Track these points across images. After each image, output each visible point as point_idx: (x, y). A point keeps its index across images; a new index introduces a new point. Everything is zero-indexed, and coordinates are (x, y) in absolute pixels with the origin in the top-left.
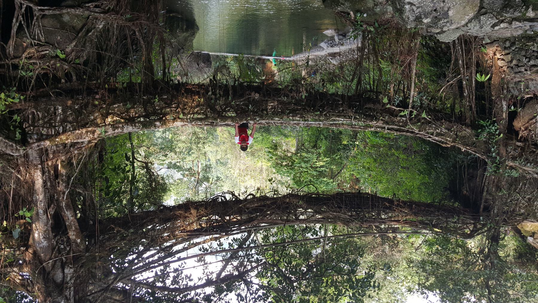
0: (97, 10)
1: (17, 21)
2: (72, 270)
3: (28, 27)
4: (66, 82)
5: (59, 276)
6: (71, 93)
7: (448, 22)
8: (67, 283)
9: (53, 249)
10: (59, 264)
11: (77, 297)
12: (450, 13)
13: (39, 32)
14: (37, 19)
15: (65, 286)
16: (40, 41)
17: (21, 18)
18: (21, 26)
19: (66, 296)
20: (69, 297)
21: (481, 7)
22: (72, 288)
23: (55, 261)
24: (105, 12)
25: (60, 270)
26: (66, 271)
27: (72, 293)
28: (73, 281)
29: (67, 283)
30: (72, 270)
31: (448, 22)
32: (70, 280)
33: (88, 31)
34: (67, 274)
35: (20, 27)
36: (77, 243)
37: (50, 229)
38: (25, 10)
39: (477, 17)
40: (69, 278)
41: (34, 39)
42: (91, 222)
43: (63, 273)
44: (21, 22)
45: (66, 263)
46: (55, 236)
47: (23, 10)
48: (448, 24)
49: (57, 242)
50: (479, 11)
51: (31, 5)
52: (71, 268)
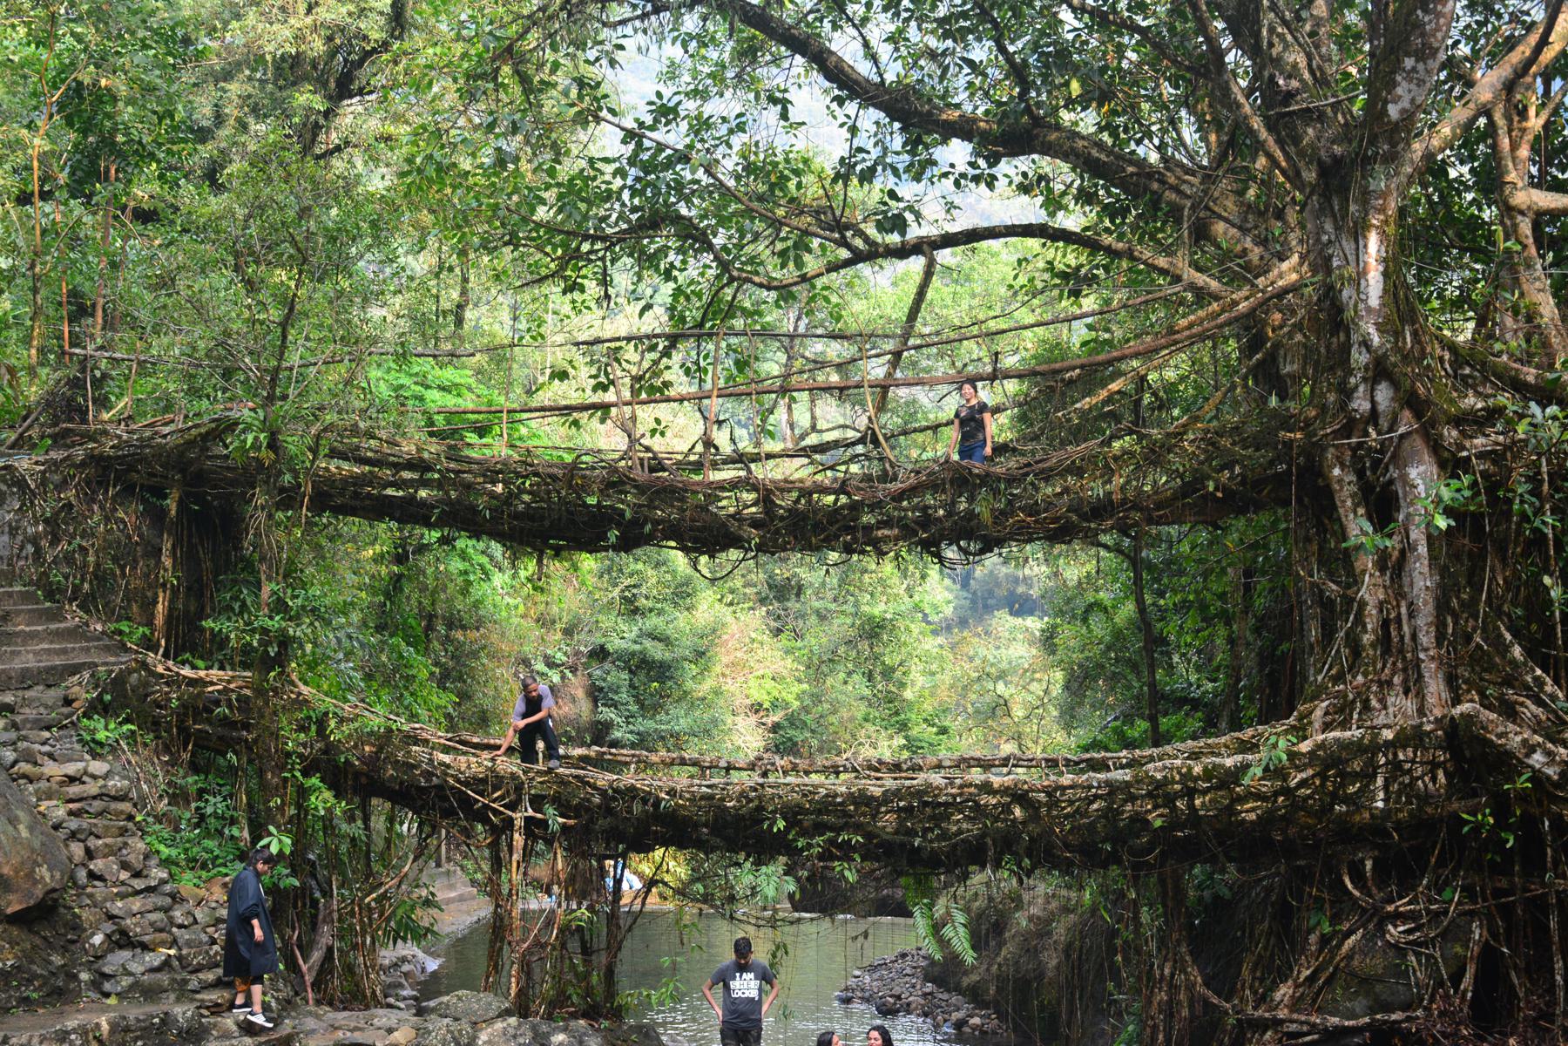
0: (1294, 1027)
1: (1466, 991)
2: (1355, 405)
4: (1362, 862)
5: (1384, 394)
6: (1349, 835)
7: (515, 1037)
8: (1364, 379)
10: (1384, 423)
11: (1342, 337)
15: (1370, 374)
16: (1418, 955)
23: (1391, 430)
24: (1278, 1023)
26: (1366, 406)
28: (1353, 380)
29: (1364, 379)
30: (1355, 405)
31: (515, 1037)
32: (1357, 387)
33: (1311, 979)
35: (1456, 978)
40: (1361, 389)
41: (1429, 957)
42: (1306, 500)
44: (1456, 992)
45: (1367, 423)
46: (1391, 482)
48: (511, 1031)
49: (1387, 470)
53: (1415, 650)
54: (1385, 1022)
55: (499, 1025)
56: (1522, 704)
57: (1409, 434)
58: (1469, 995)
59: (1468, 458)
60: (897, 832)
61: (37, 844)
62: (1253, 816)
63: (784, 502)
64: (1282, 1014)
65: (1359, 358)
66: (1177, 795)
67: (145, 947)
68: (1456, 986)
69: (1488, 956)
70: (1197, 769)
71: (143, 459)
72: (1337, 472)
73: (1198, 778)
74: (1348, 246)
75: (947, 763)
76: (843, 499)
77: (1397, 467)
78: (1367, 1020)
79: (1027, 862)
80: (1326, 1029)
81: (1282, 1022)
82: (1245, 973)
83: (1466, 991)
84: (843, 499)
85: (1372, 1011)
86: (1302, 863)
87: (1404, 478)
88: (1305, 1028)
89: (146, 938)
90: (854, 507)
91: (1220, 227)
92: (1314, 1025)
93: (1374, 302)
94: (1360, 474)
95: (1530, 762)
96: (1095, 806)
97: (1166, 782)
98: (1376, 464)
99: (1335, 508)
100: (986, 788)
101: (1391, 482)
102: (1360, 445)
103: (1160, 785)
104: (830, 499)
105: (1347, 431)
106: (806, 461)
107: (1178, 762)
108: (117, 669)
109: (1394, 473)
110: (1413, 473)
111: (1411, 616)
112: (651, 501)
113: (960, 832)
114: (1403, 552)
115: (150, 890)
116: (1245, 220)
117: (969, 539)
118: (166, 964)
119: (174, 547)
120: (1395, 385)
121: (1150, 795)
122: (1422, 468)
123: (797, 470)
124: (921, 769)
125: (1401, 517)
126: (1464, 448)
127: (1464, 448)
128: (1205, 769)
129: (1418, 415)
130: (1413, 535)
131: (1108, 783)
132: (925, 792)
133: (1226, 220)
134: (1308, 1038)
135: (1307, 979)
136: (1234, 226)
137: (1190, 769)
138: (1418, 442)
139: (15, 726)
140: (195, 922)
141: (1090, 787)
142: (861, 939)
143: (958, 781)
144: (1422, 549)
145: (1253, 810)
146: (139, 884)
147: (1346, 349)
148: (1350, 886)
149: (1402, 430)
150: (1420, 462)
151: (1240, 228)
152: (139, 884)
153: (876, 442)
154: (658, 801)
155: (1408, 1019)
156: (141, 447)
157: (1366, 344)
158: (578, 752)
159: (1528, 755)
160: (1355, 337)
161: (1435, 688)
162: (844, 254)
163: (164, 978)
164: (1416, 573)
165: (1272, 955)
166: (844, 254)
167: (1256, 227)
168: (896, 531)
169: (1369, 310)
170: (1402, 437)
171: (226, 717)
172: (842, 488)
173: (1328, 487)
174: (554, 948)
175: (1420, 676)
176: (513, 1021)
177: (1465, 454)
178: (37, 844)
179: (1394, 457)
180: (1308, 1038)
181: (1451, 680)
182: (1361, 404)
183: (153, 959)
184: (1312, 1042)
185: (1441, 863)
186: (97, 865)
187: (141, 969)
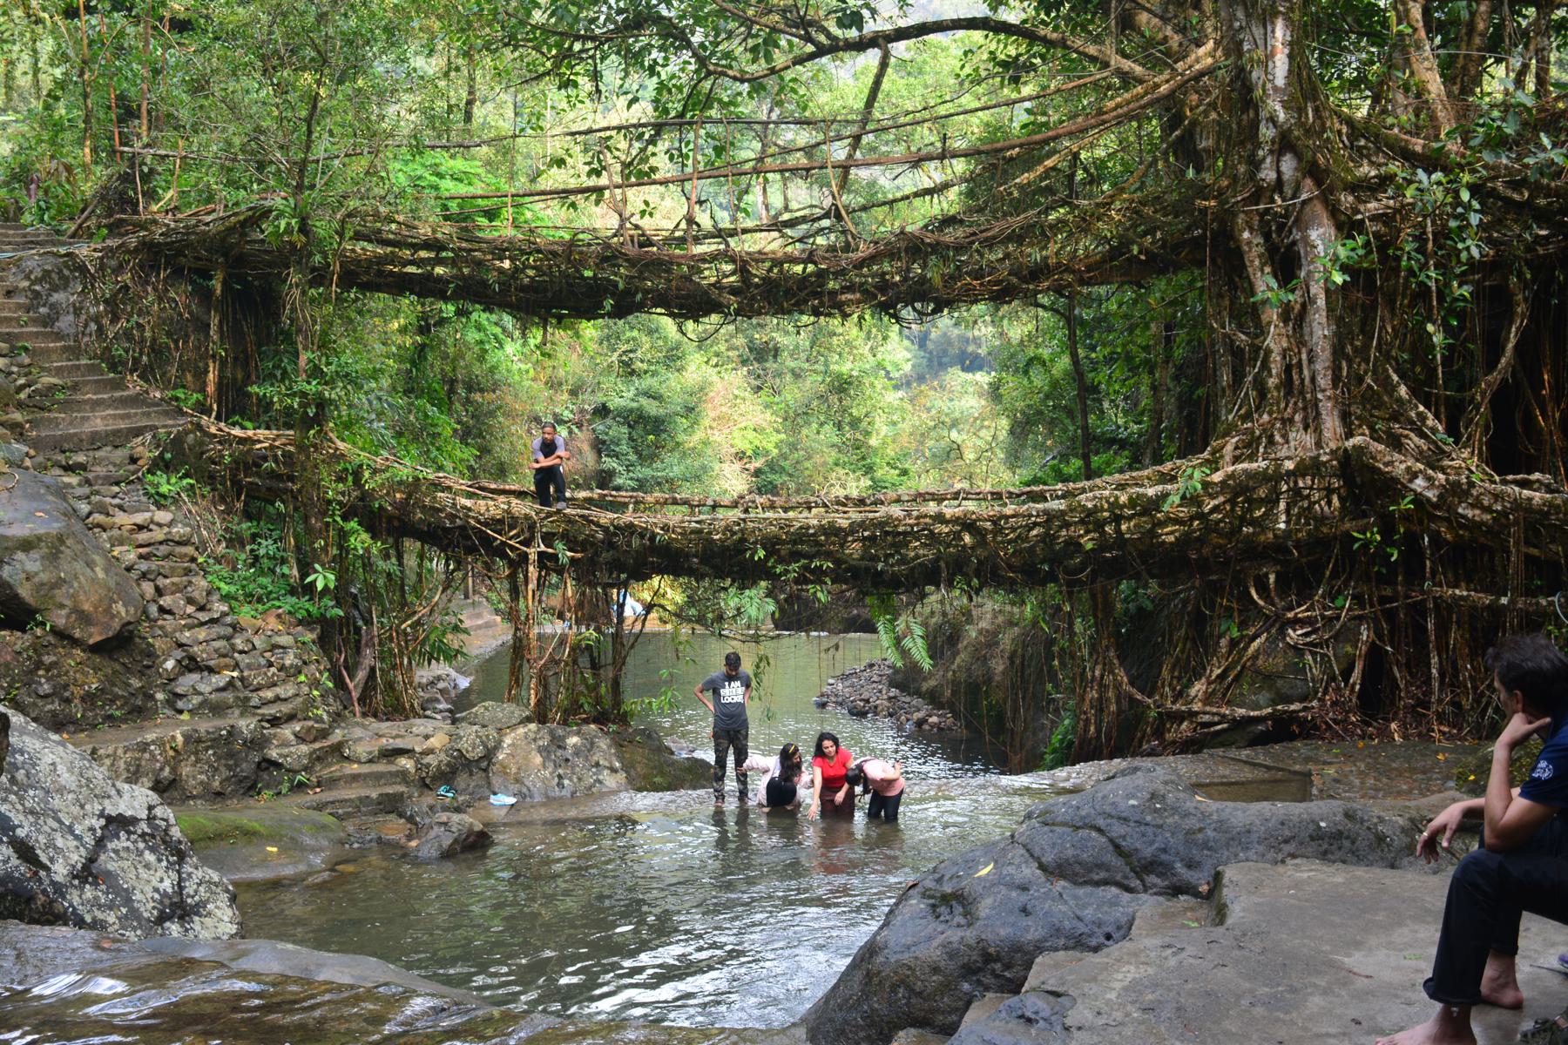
0: (1206, 718)
1: (1354, 685)
2: (1262, 175)
4: (1266, 575)
5: (1288, 165)
6: (1256, 553)
7: (535, 740)
8: (1271, 152)
10: (1288, 191)
12: (538, 760)
16: (1314, 654)
21: (485, 770)
23: (1294, 197)
24: (1192, 715)
25: (1286, 177)
26: (1273, 175)
28: (1261, 153)
29: (1271, 152)
30: (1262, 175)
31: (535, 740)
32: (1264, 158)
33: (1222, 677)
35: (1346, 674)
36: (1251, 230)
37: (1304, 261)
39: (489, 755)
40: (1268, 160)
41: (1323, 656)
42: (1219, 261)
45: (1274, 191)
46: (1294, 243)
48: (532, 735)
49: (1290, 232)
50: (490, 763)
53: (1314, 391)
54: (1285, 712)
55: (521, 730)
56: (1407, 437)
57: (1310, 199)
59: (1362, 221)
60: (862, 558)
61: (112, 584)
62: (1171, 538)
63: (758, 271)
64: (1196, 707)
65: (1267, 132)
66: (1105, 522)
67: (211, 670)
68: (1346, 681)
69: (1374, 654)
70: (1123, 499)
71: (189, 245)
72: (1246, 235)
73: (1124, 506)
74: (1258, 32)
75: (906, 498)
76: (811, 268)
77: (1299, 229)
78: (1269, 710)
79: (975, 582)
80: (1234, 719)
81: (1196, 714)
82: (1165, 673)
83: (1354, 684)
84: (811, 268)
85: (1274, 703)
86: (1214, 577)
87: (1306, 239)
88: (1216, 719)
89: (212, 663)
90: (821, 275)
91: (1143, 17)
92: (1224, 716)
93: (1280, 82)
94: (1267, 236)
95: (1413, 486)
96: (1035, 532)
97: (1096, 509)
98: (1281, 227)
99: (1244, 267)
100: (939, 518)
101: (1294, 243)
102: (1267, 211)
103: (1090, 513)
104: (799, 269)
105: (1255, 198)
106: (775, 234)
107: (1107, 493)
108: (175, 430)
109: (1296, 235)
110: (1314, 235)
111: (1311, 361)
112: (641, 273)
113: (917, 557)
114: (1304, 305)
115: (213, 621)
116: (1166, 10)
117: (922, 300)
118: (231, 684)
119: (221, 322)
120: (1299, 156)
121: (1082, 521)
122: (1321, 230)
123: (769, 243)
124: (882, 503)
125: (1303, 274)
126: (1359, 212)
127: (1359, 212)
128: (1130, 498)
129: (1318, 183)
130: (1313, 291)
131: (1046, 512)
132: (886, 523)
133: (1149, 11)
134: (1219, 727)
135: (1218, 676)
136: (1156, 16)
137: (1117, 498)
138: (1318, 208)
139: (88, 482)
140: (254, 648)
141: (1030, 516)
142: (832, 651)
143: (915, 513)
144: (1321, 302)
145: (1172, 533)
146: (203, 616)
147: (1255, 125)
148: (1255, 597)
149: (1304, 196)
150: (1320, 225)
151: (1161, 18)
152: (203, 616)
153: (839, 217)
154: (654, 535)
155: (1305, 709)
156: (187, 234)
157: (1272, 119)
158: (582, 494)
159: (1411, 481)
160: (1263, 114)
161: (1331, 423)
162: (810, 48)
163: (229, 696)
164: (1315, 324)
165: (1188, 657)
166: (810, 48)
167: (1176, 16)
168: (858, 295)
169: (1276, 89)
170: (1304, 202)
171: (273, 471)
172: (810, 258)
173: (1239, 248)
174: (567, 664)
175: (1318, 414)
176: (533, 726)
177: (1359, 217)
178: (112, 584)
179: (1297, 220)
180: (1219, 727)
181: (1345, 417)
183: (219, 680)
184: (1223, 730)
185: (1335, 575)
186: (166, 601)
187: (209, 689)
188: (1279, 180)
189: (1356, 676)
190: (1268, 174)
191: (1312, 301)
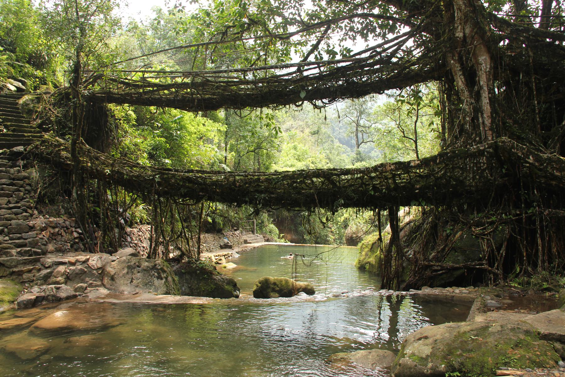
0: (436, 268)
1: (502, 254)
2: (457, 35)
3: (493, 250)
9: (474, 54)
10: (469, 41)
13: (484, 246)
14: (485, 257)
17: (499, 258)
18: (499, 251)
19: (461, 11)
20: (459, 12)
22: (456, 19)
26: (461, 35)
27: (456, 15)
28: (456, 25)
30: (457, 35)
32: (458, 27)
34: (461, 32)
35: (499, 249)
36: (454, 60)
38: (495, 264)
40: (459, 28)
43: (464, 33)
44: (498, 254)
46: (473, 66)
47: (496, 264)
51: (490, 268)
52: (458, 37)
58: (504, 254)
81: (432, 265)
101: (473, 66)
122: (483, 58)
130: (482, 83)
144: (485, 88)
150: (483, 55)
164: (483, 98)
182: (459, 34)
188: (464, 36)
189: (503, 251)
190: (459, 34)
191: (481, 88)
